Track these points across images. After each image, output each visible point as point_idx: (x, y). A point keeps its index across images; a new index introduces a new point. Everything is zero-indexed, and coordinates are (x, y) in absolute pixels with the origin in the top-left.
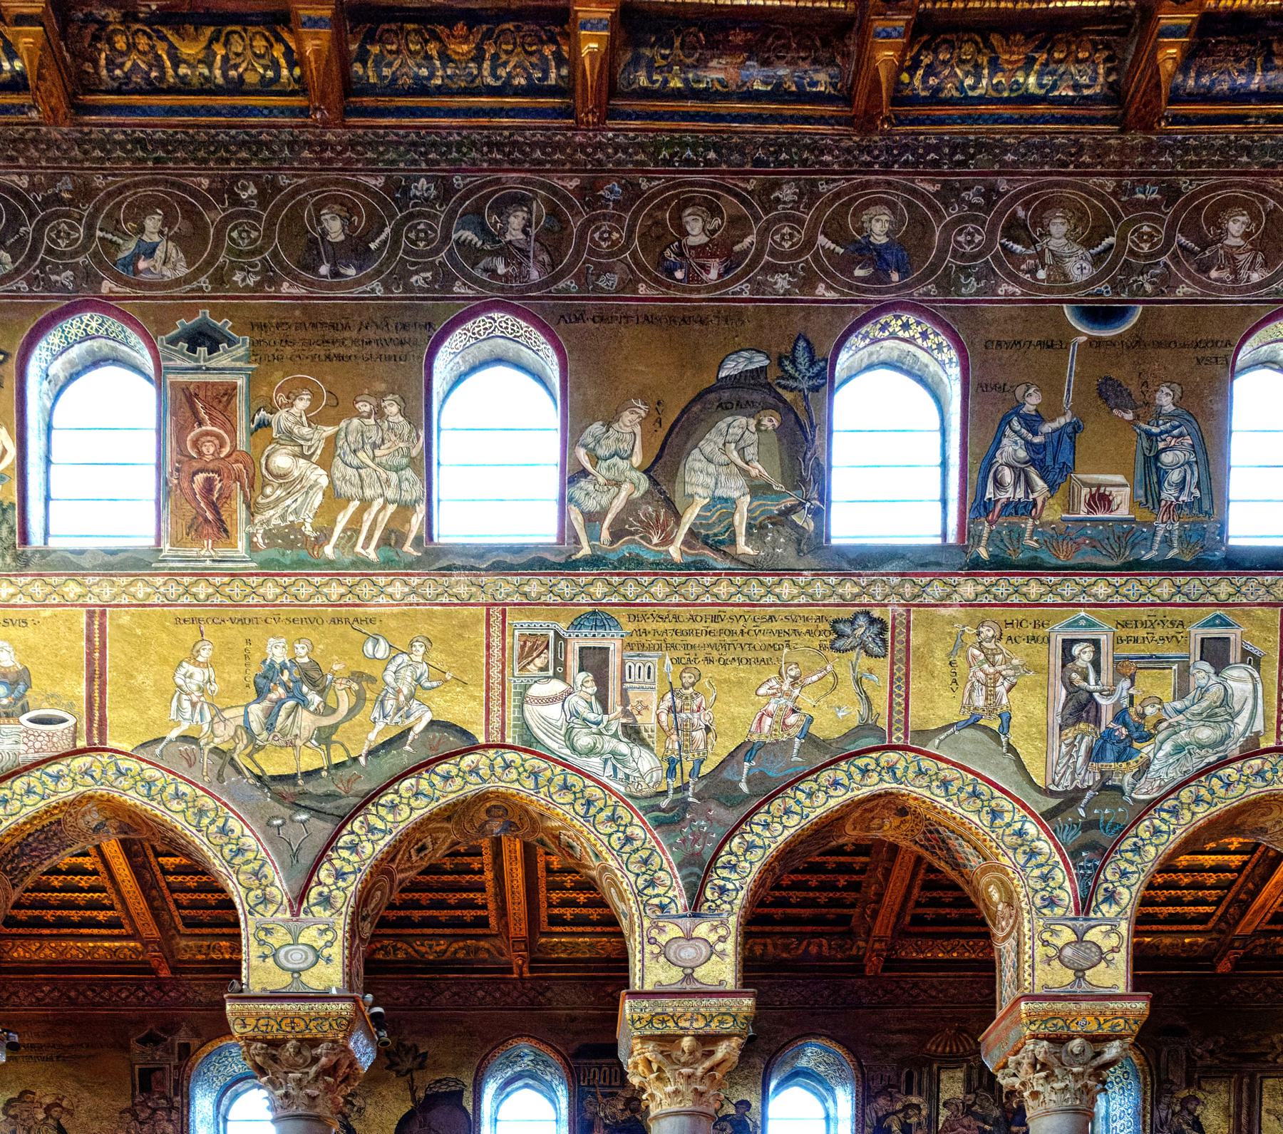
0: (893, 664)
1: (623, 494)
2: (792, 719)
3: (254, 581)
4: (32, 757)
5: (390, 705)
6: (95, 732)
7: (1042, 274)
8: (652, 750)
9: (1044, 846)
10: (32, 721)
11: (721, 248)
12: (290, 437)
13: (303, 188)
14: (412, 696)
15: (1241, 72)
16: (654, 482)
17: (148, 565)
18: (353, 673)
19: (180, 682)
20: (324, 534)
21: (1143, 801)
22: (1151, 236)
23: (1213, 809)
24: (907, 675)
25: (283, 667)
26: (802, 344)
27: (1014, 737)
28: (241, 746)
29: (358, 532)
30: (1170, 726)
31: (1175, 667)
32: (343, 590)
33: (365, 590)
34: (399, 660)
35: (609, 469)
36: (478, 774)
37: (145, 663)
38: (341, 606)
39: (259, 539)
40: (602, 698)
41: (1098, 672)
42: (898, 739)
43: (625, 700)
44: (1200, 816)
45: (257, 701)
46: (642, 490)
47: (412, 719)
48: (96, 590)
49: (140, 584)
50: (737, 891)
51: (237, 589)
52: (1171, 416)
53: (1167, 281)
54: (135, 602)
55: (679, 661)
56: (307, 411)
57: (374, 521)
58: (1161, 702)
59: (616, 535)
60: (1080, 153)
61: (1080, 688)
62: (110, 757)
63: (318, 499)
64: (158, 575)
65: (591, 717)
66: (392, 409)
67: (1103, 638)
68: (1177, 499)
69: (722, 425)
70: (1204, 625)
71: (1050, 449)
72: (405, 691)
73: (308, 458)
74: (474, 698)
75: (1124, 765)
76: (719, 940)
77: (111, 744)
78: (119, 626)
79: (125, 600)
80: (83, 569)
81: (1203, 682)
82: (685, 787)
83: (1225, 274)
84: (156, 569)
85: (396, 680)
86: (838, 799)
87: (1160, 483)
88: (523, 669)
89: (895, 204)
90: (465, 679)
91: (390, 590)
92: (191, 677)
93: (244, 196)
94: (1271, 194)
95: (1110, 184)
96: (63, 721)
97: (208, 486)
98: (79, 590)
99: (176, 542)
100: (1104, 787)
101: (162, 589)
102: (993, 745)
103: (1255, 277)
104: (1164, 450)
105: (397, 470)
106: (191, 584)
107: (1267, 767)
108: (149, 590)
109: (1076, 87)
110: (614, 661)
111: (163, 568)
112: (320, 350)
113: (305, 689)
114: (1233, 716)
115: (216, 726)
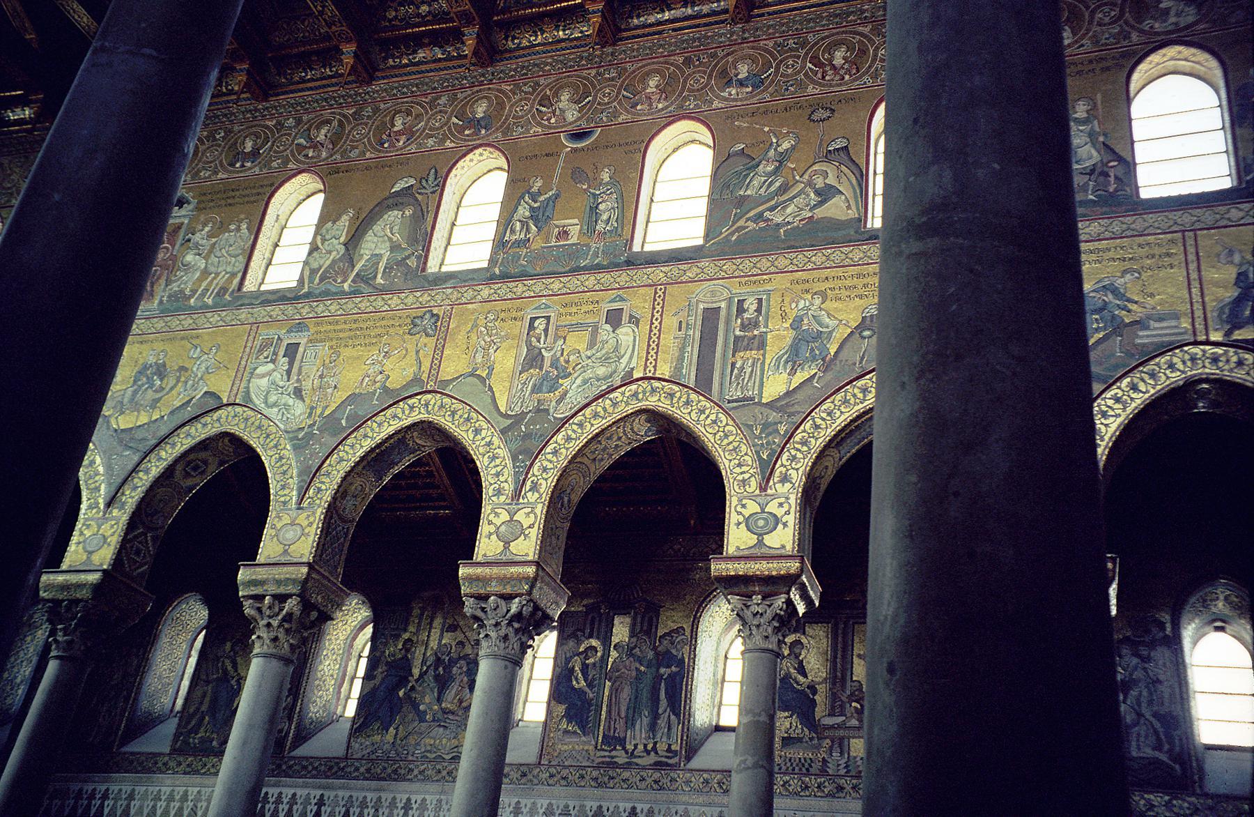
0: (438, 340)
1: (332, 257)
2: (379, 377)
7: (553, 120)
8: (304, 401)
9: (503, 452)
11: (409, 132)
12: (197, 245)
13: (242, 130)
15: (658, 13)
16: (347, 249)
20: (194, 292)
21: (560, 418)
22: (610, 94)
23: (604, 421)
24: (444, 346)
26: (433, 170)
27: (493, 381)
29: (208, 290)
30: (583, 367)
31: (590, 329)
35: (329, 245)
40: (289, 372)
41: (546, 336)
42: (431, 386)
43: (299, 373)
44: (596, 426)
46: (341, 253)
50: (326, 490)
52: (608, 183)
53: (616, 114)
55: (332, 347)
57: (217, 284)
58: (579, 352)
59: (321, 280)
60: (581, 60)
61: (534, 347)
65: (281, 384)
66: (244, 226)
67: (553, 315)
68: (604, 229)
69: (386, 217)
70: (610, 302)
71: (541, 210)
73: (199, 255)
75: (552, 394)
76: (308, 525)
81: (605, 337)
82: (313, 425)
83: (645, 106)
85: (198, 369)
86: (395, 426)
87: (596, 222)
88: (257, 358)
89: (491, 97)
90: (228, 366)
93: (218, 137)
94: (672, 65)
95: (593, 72)
100: (538, 411)
102: (480, 386)
103: (660, 106)
104: (601, 203)
105: (235, 256)
107: (640, 390)
109: (582, 32)
110: (301, 349)
112: (223, 202)
114: (620, 358)
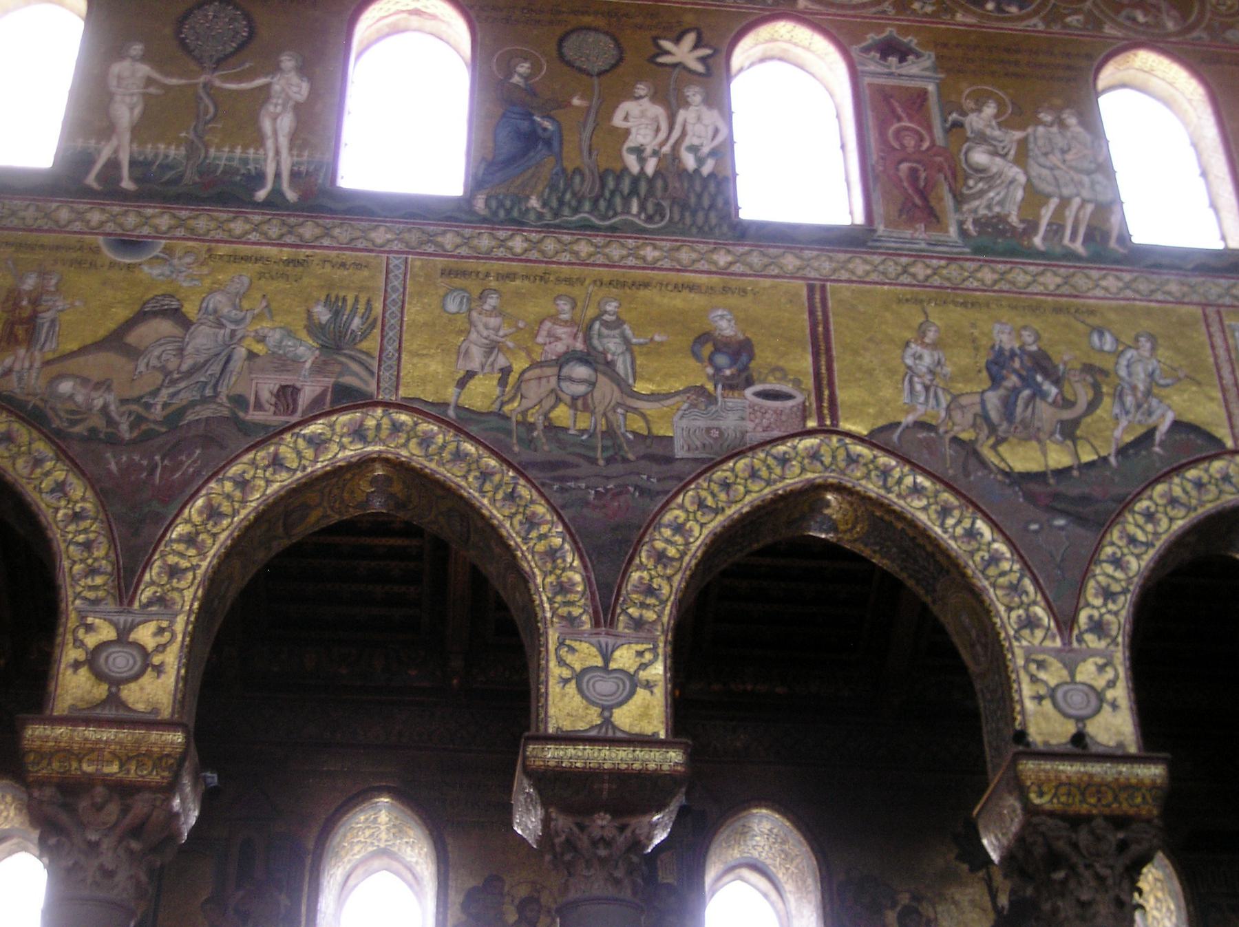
3: (971, 266)
4: (762, 436)
5: (1129, 400)
6: (826, 412)
10: (758, 394)
12: (982, 138)
14: (1148, 393)
18: (1085, 365)
19: (909, 361)
20: (1032, 227)
25: (1013, 354)
28: (983, 436)
32: (1058, 280)
33: (1080, 281)
34: (1129, 354)
36: (1230, 482)
37: (871, 340)
38: (1060, 296)
39: (969, 226)
45: (990, 389)
47: (1154, 417)
48: (816, 264)
49: (858, 261)
51: (953, 271)
54: (854, 278)
56: (996, 116)
63: (1019, 194)
64: (874, 253)
72: (1141, 387)
73: (1004, 156)
74: (1212, 399)
77: (845, 426)
79: (845, 275)
80: (800, 242)
84: (871, 247)
85: (1130, 374)
91: (1104, 283)
92: (920, 357)
96: (789, 397)
97: (913, 173)
98: (798, 263)
99: (889, 223)
101: (881, 268)
105: (1089, 173)
106: (908, 265)
108: (868, 268)
113: (1039, 378)
115: (953, 413)
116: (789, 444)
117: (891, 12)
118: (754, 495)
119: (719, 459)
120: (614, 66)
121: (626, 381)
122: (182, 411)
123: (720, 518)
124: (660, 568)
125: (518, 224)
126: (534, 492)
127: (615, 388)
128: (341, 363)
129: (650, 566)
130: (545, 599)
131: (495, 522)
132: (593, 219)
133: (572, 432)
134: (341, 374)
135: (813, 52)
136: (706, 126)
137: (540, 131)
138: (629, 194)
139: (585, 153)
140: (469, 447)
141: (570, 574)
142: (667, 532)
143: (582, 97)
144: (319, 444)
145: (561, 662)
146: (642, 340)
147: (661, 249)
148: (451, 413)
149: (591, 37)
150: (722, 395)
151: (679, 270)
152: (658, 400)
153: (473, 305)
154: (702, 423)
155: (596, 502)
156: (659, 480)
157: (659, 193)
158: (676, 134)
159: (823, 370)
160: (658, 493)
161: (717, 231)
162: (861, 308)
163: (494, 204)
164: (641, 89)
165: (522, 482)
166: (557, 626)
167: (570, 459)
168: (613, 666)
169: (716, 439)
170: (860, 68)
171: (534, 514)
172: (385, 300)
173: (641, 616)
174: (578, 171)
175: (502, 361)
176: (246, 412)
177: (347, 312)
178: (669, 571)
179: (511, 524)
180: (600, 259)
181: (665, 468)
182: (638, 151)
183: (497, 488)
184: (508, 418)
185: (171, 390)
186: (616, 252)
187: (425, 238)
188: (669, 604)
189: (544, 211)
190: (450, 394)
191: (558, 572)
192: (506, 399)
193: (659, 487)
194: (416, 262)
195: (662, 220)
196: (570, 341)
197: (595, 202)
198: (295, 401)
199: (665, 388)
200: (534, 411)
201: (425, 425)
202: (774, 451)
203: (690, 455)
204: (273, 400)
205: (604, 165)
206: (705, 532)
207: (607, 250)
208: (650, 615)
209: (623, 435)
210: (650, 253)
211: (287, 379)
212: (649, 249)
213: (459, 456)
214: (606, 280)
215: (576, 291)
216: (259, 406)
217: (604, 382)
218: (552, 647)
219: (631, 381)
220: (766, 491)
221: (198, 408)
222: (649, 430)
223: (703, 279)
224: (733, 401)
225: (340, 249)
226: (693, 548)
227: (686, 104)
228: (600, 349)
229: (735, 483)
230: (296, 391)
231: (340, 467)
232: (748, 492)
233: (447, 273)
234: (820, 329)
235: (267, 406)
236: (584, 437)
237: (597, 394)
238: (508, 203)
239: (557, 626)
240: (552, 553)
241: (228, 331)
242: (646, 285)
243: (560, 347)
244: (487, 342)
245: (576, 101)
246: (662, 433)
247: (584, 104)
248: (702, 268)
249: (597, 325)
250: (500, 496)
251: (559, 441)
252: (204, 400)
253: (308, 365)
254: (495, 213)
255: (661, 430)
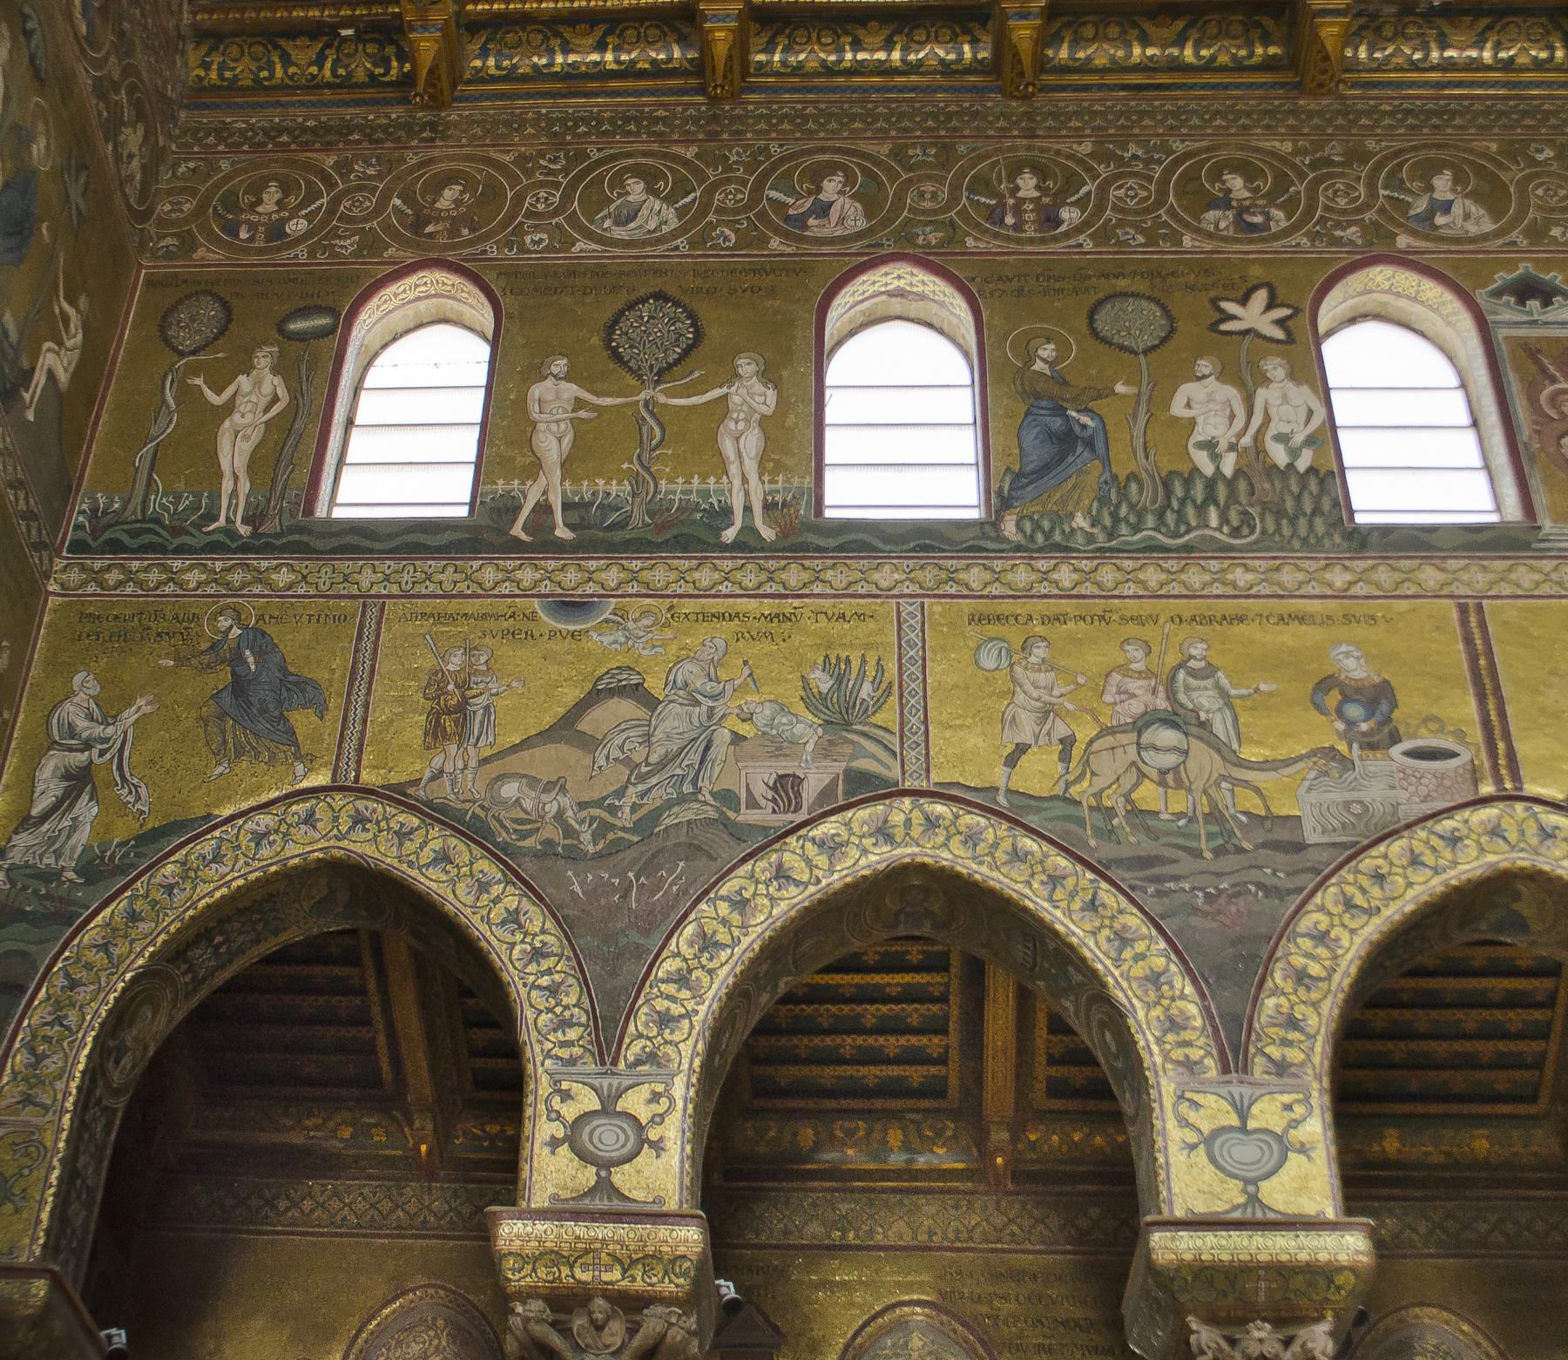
17: (1526, 546)
37: (1553, 673)
48: (1465, 577)
54: (1520, 592)
62: (1527, 809)
77: (1531, 789)
78: (1505, 623)
79: (1507, 590)
96: (1454, 755)
98: (1441, 576)
101: (1554, 576)
108: (1537, 577)
111: (1549, 550)
116: (1458, 817)
117: (1523, 243)
118: (1418, 889)
119: (1365, 842)
120: (1164, 340)
121: (1229, 747)
122: (656, 815)
123: (1376, 921)
124: (1302, 991)
125: (1063, 550)
126: (1121, 898)
127: (1216, 756)
128: (852, 742)
129: (1288, 989)
130: (1151, 1038)
131: (1074, 940)
132: (1160, 537)
133: (1164, 816)
134: (853, 757)
135: (1422, 303)
136: (1295, 407)
137: (1077, 429)
138: (1204, 502)
139: (1140, 453)
140: (1028, 843)
141: (1180, 1003)
142: (1306, 944)
143: (1126, 383)
144: (835, 849)
145: (1184, 1123)
146: (1244, 691)
147: (1255, 570)
148: (1002, 799)
149: (1130, 305)
150: (1360, 757)
151: (1281, 597)
152: (1275, 770)
153: (1015, 658)
154: (1338, 796)
155: (1207, 908)
156: (1288, 874)
157: (1244, 500)
158: (1257, 420)
159: (1493, 716)
160: (1289, 892)
161: (1327, 544)
162: (1534, 631)
163: (1028, 527)
164: (1204, 366)
165: (1104, 885)
166: (1171, 1073)
167: (1168, 853)
168: (1252, 1124)
169: (1358, 816)
170: (1490, 318)
171: (1124, 927)
172: (900, 659)
173: (1284, 1057)
174: (1133, 477)
175: (1061, 730)
176: (737, 811)
177: (853, 676)
178: (1315, 996)
179: (1097, 943)
180: (1177, 589)
181: (1295, 857)
182: (1210, 446)
183: (1072, 896)
184: (1077, 803)
185: (641, 787)
186: (1195, 578)
187: (944, 575)
188: (1320, 1038)
189: (1095, 531)
190: (998, 775)
191: (1166, 1002)
192: (1071, 777)
193: (1289, 884)
194: (935, 607)
195: (1252, 532)
196: (1149, 698)
197: (1161, 516)
198: (798, 794)
199: (1282, 753)
200: (1110, 791)
201: (968, 817)
202: (1438, 828)
203: (1325, 839)
204: (770, 794)
205: (1166, 466)
206: (1358, 940)
207: (1183, 577)
208: (1295, 1055)
209: (1234, 818)
210: (1241, 577)
211: (785, 766)
212: (1239, 571)
213: (1017, 856)
214: (1186, 615)
215: (1148, 632)
216: (753, 804)
217: (1198, 748)
218: (1168, 1103)
219: (1235, 746)
220: (1435, 881)
221: (676, 809)
222: (1268, 808)
223: (1316, 606)
224: (1375, 764)
225: (835, 596)
226: (1344, 963)
227: (1265, 381)
228: (1191, 706)
229: (1390, 874)
230: (798, 781)
231: (864, 877)
232: (1410, 884)
233: (977, 619)
234: (1482, 662)
235: (763, 802)
236: (1182, 823)
237: (1191, 764)
238: (1046, 524)
239: (1171, 1073)
240: (1155, 979)
241: (704, 708)
242: (1241, 619)
243: (1136, 707)
244: (1038, 704)
245: (1120, 388)
246: (1284, 812)
247: (1132, 390)
248: (1313, 592)
249: (1181, 675)
250: (1077, 905)
251: (1148, 830)
252: (682, 799)
253: (810, 747)
254: (1032, 538)
255: (1283, 808)
